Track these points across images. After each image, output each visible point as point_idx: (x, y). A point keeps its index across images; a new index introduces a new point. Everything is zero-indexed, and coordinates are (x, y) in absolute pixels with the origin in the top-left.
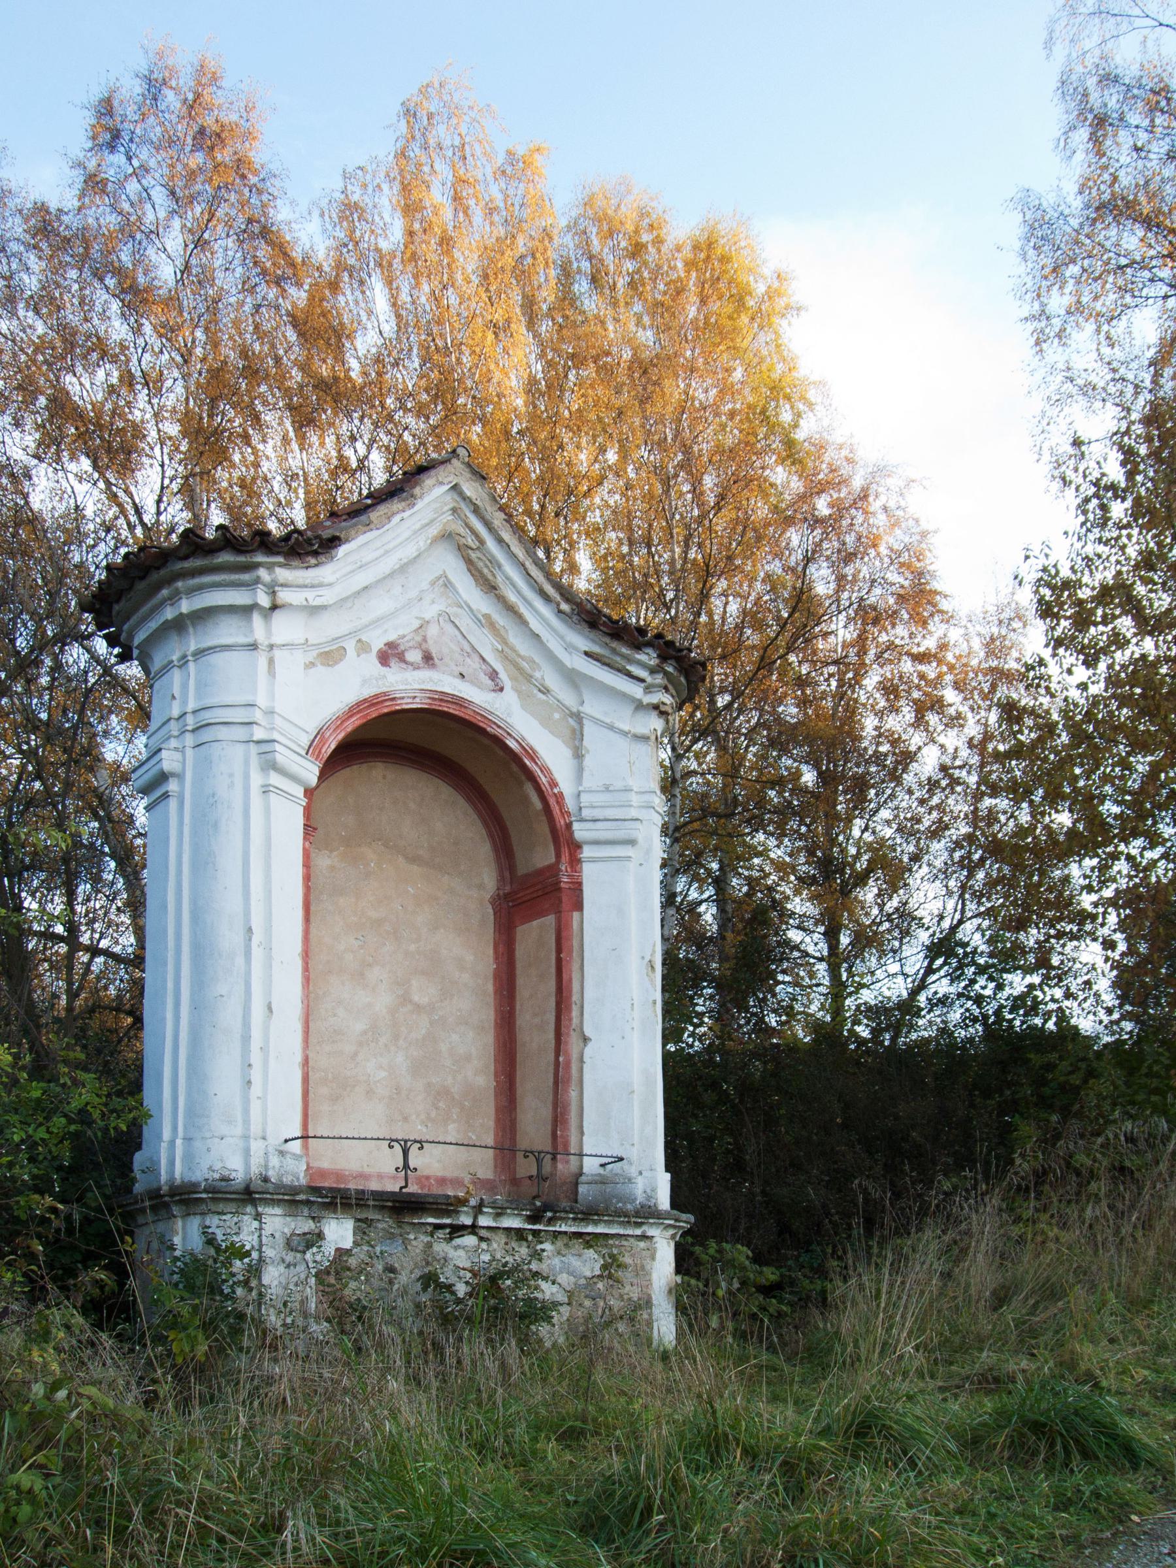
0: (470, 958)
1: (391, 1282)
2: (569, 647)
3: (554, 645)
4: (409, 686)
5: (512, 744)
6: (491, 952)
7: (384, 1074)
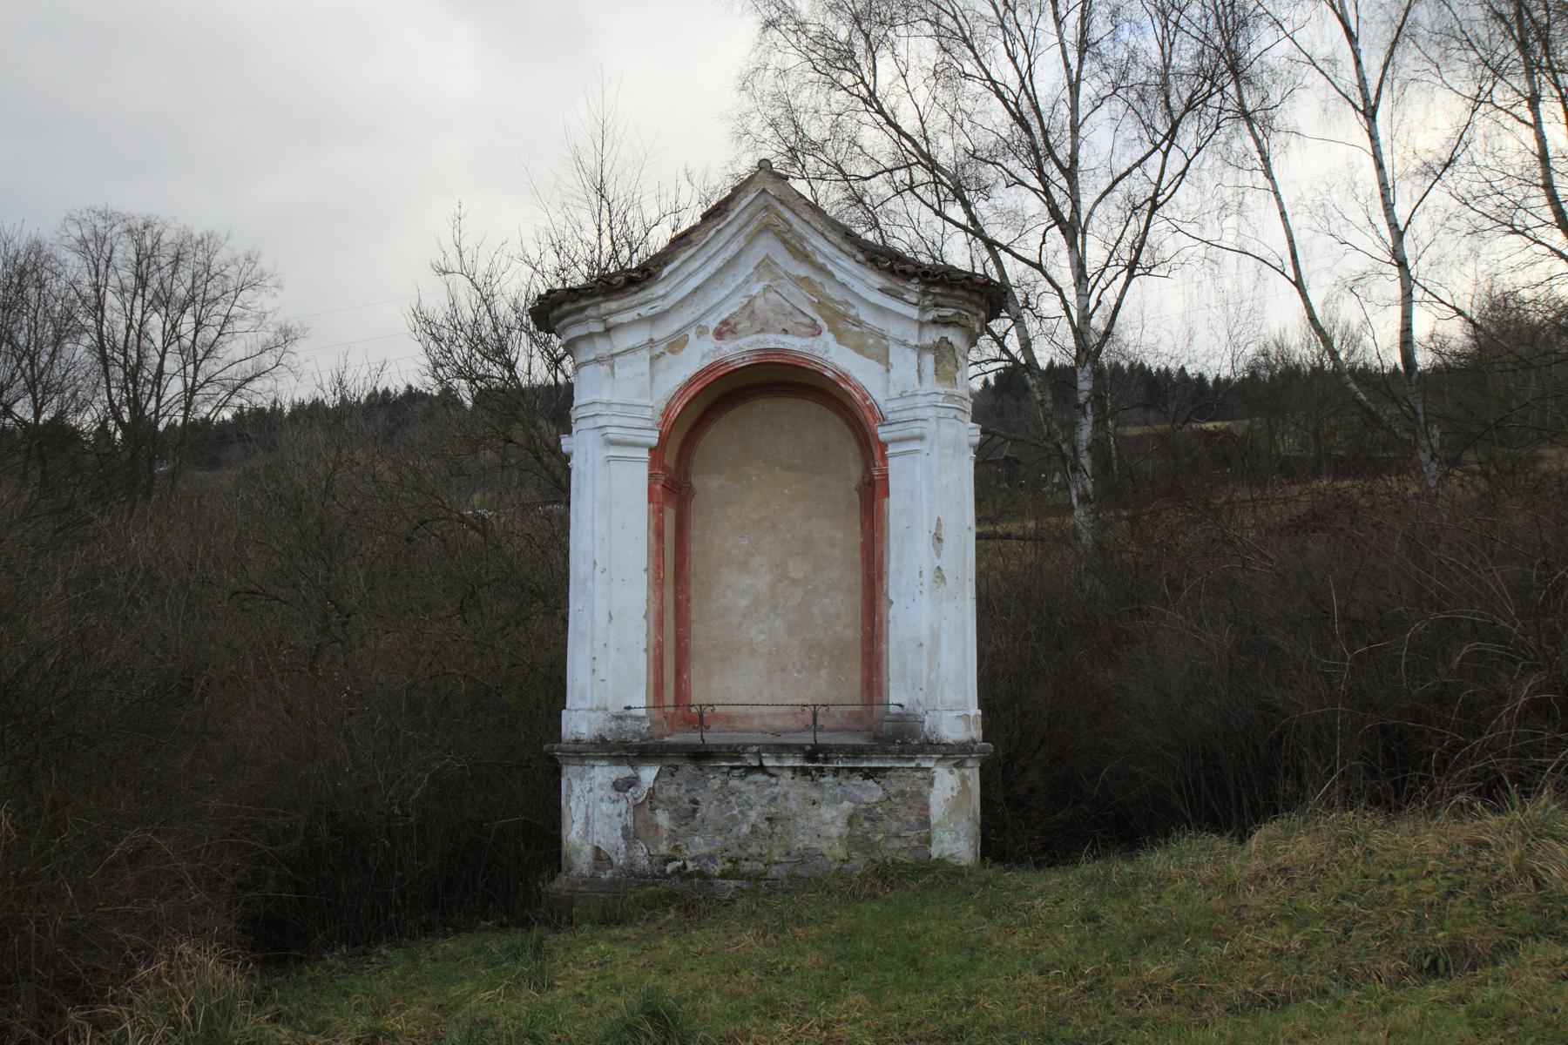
0: (839, 535)
1: (695, 811)
2: (870, 287)
3: (859, 288)
4: (738, 350)
5: (829, 374)
6: (858, 528)
7: (763, 637)
